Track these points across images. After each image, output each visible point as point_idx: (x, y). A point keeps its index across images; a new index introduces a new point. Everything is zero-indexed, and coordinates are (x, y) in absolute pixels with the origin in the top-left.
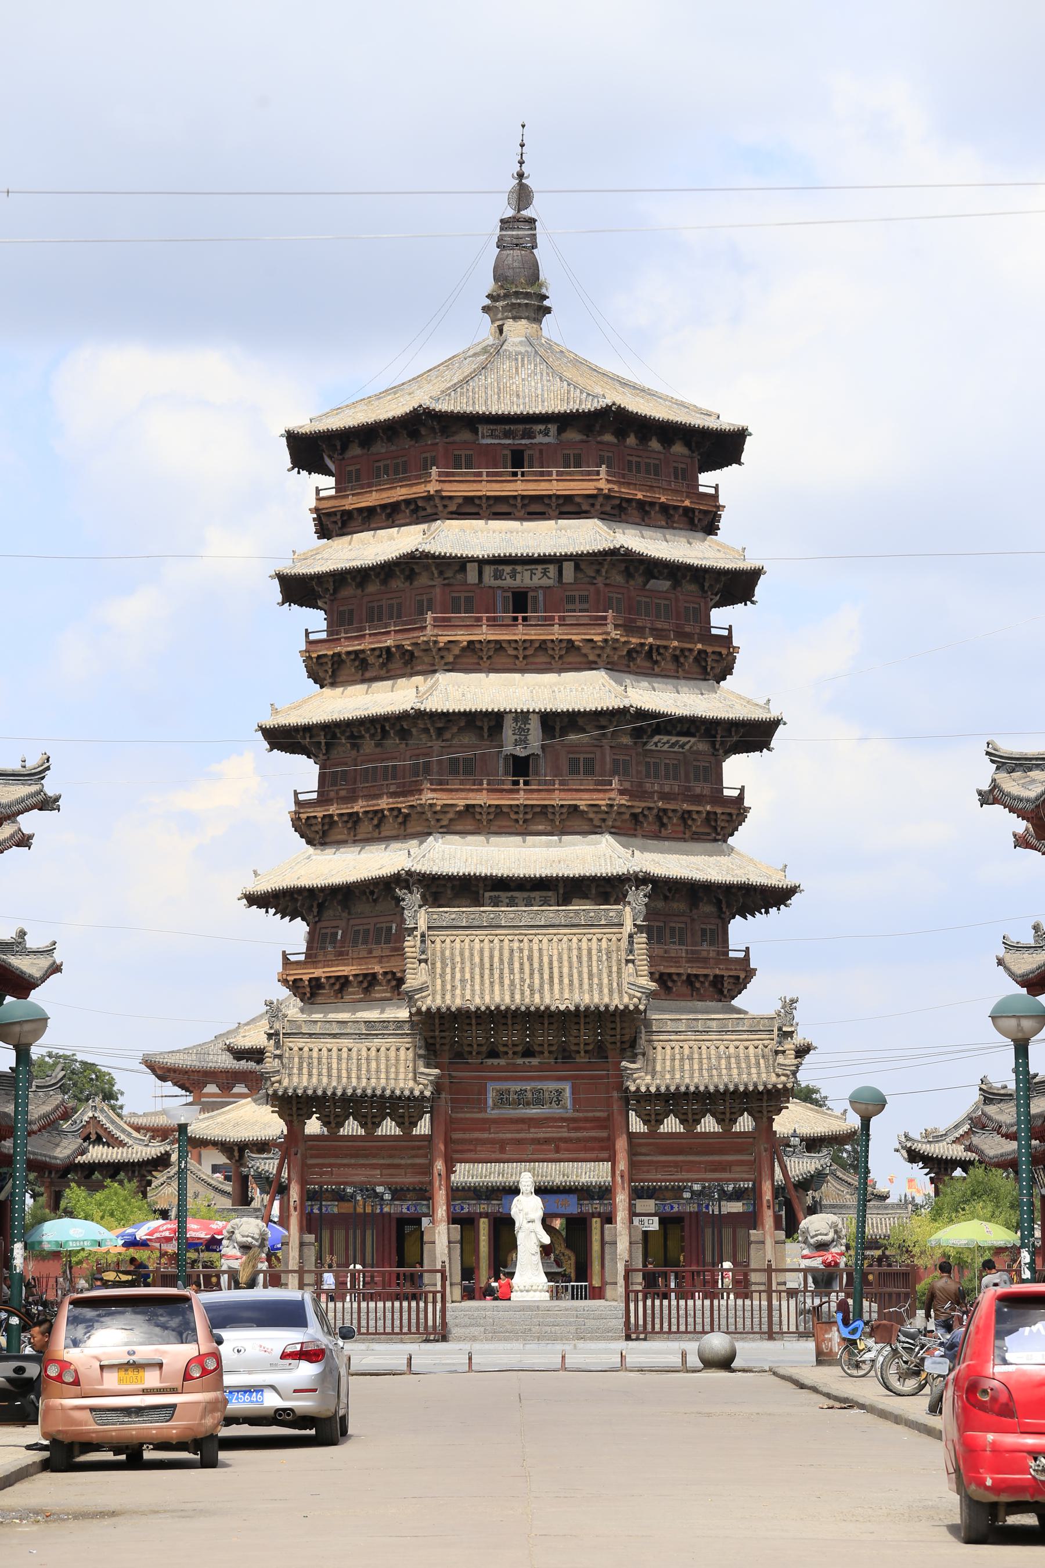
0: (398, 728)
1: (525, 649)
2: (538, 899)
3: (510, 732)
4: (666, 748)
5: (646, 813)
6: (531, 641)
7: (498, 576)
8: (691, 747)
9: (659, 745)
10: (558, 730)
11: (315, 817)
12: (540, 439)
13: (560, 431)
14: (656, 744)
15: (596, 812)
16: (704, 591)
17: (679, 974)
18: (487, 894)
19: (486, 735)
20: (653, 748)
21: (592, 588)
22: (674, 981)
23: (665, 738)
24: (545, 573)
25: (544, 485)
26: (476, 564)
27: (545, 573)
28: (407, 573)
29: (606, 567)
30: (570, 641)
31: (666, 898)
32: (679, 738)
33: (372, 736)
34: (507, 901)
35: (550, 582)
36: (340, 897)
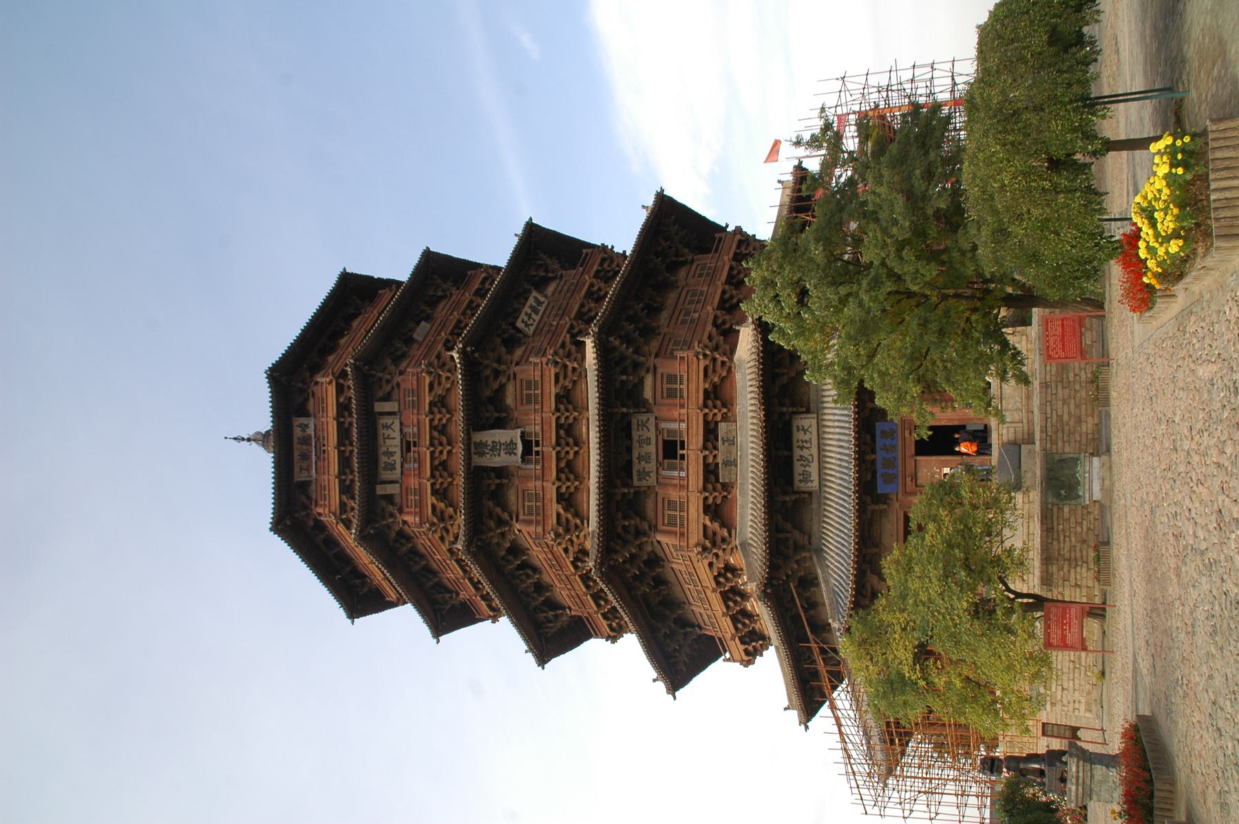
0: (511, 558)
1: (441, 444)
3: (497, 459)
4: (537, 318)
5: (576, 330)
6: (432, 438)
7: (391, 467)
8: (546, 296)
9: (531, 322)
10: (496, 415)
11: (610, 626)
12: (311, 431)
13: (304, 413)
14: (527, 325)
15: (565, 377)
16: (445, 297)
17: (724, 292)
18: (636, 483)
19: (505, 481)
20: (532, 328)
21: (402, 387)
22: (732, 297)
23: (523, 316)
24: (387, 427)
25: (330, 428)
26: (378, 487)
27: (387, 427)
28: (403, 541)
29: (380, 375)
30: (432, 404)
31: (659, 310)
32: (528, 304)
33: (528, 576)
35: (397, 423)
36: (667, 613)
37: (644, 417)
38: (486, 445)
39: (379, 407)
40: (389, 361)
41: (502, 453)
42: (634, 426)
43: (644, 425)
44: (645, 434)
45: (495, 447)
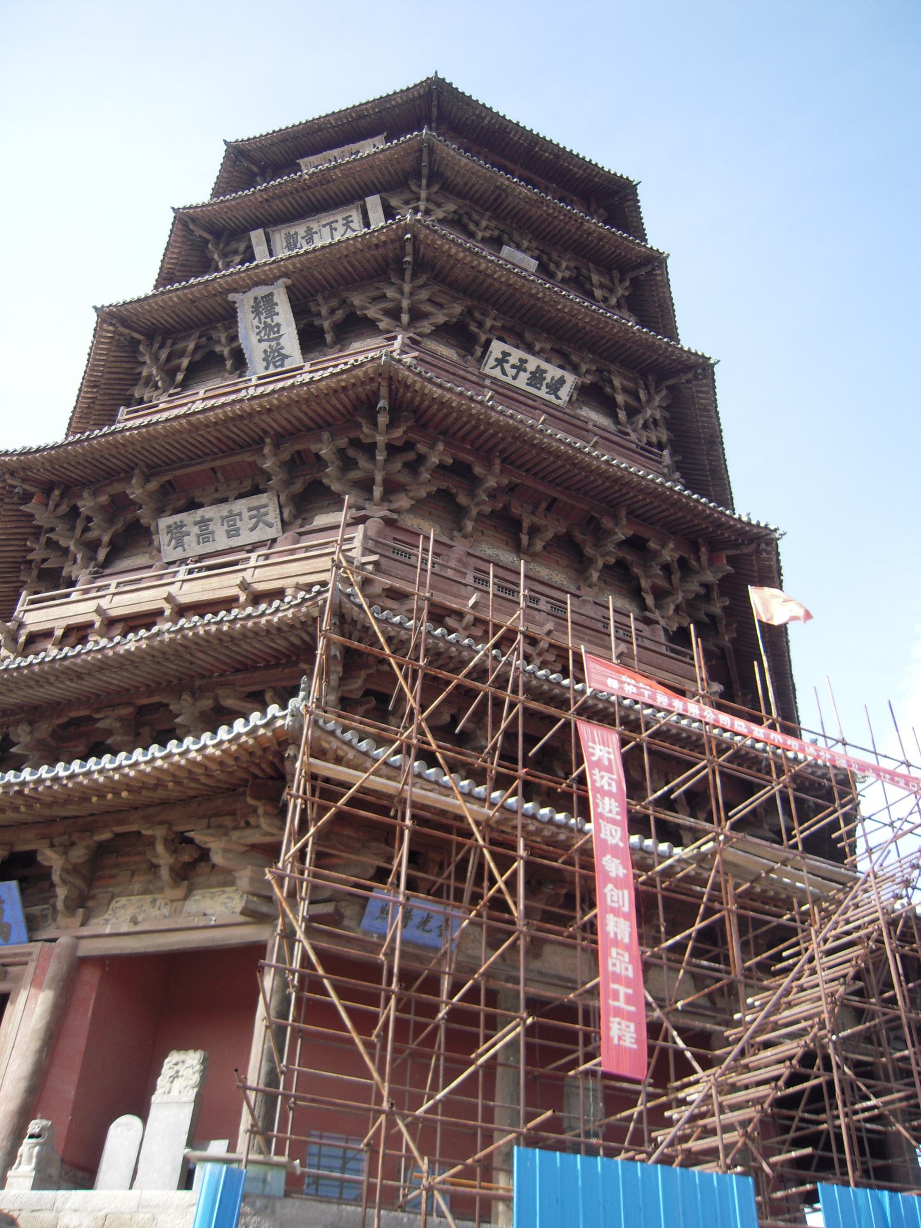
2: (246, 515)
3: (254, 338)
9: (507, 366)
18: (165, 522)
20: (497, 373)
23: (516, 355)
24: (347, 224)
26: (261, 231)
27: (347, 225)
29: (423, 195)
32: (544, 365)
34: (196, 530)
37: (273, 515)
38: (272, 313)
39: (374, 203)
40: (451, 207)
41: (265, 345)
42: (256, 500)
43: (259, 519)
44: (245, 524)
45: (271, 331)
